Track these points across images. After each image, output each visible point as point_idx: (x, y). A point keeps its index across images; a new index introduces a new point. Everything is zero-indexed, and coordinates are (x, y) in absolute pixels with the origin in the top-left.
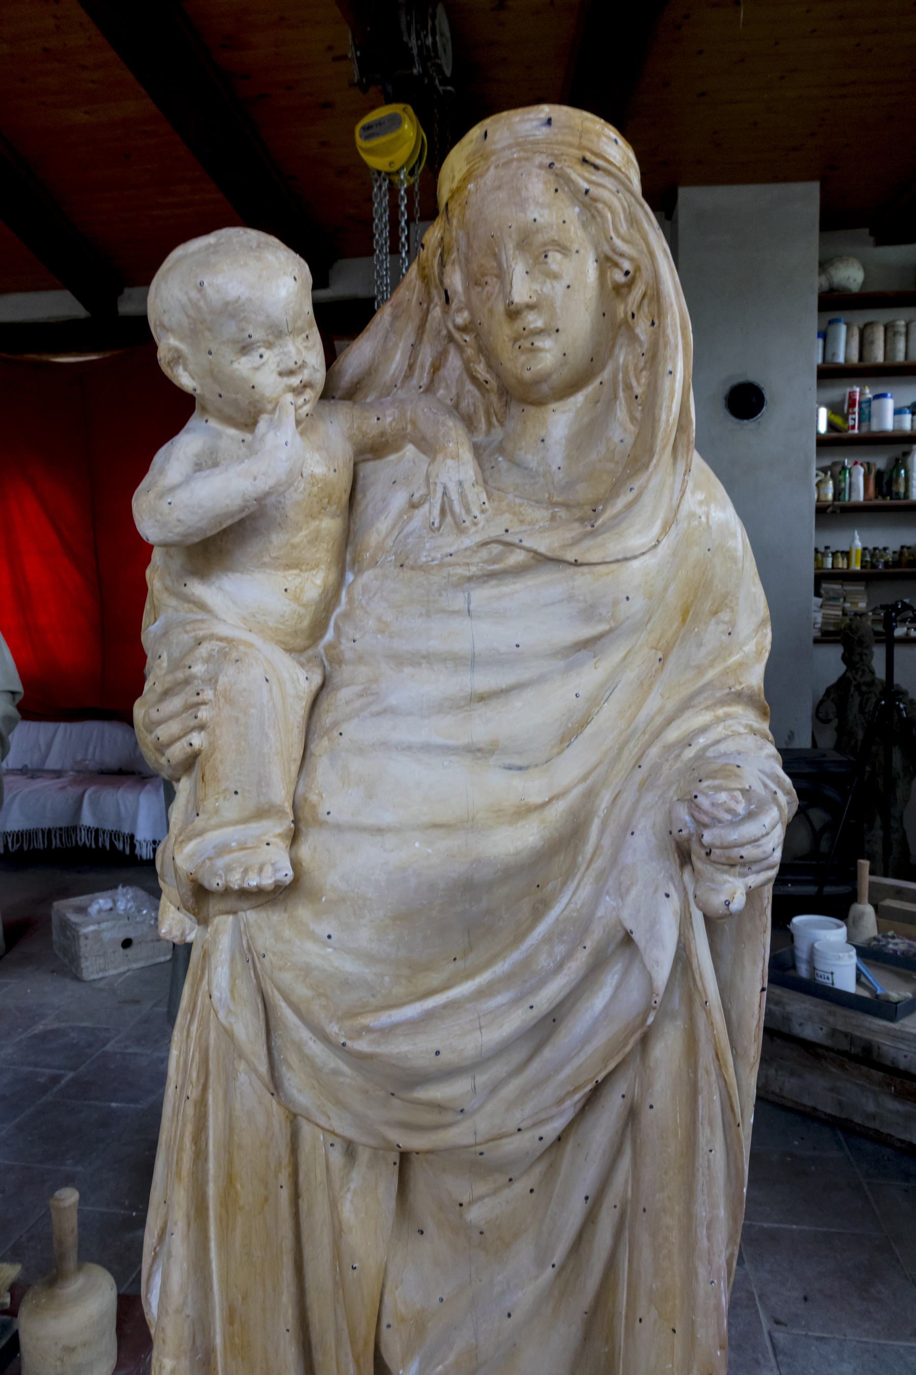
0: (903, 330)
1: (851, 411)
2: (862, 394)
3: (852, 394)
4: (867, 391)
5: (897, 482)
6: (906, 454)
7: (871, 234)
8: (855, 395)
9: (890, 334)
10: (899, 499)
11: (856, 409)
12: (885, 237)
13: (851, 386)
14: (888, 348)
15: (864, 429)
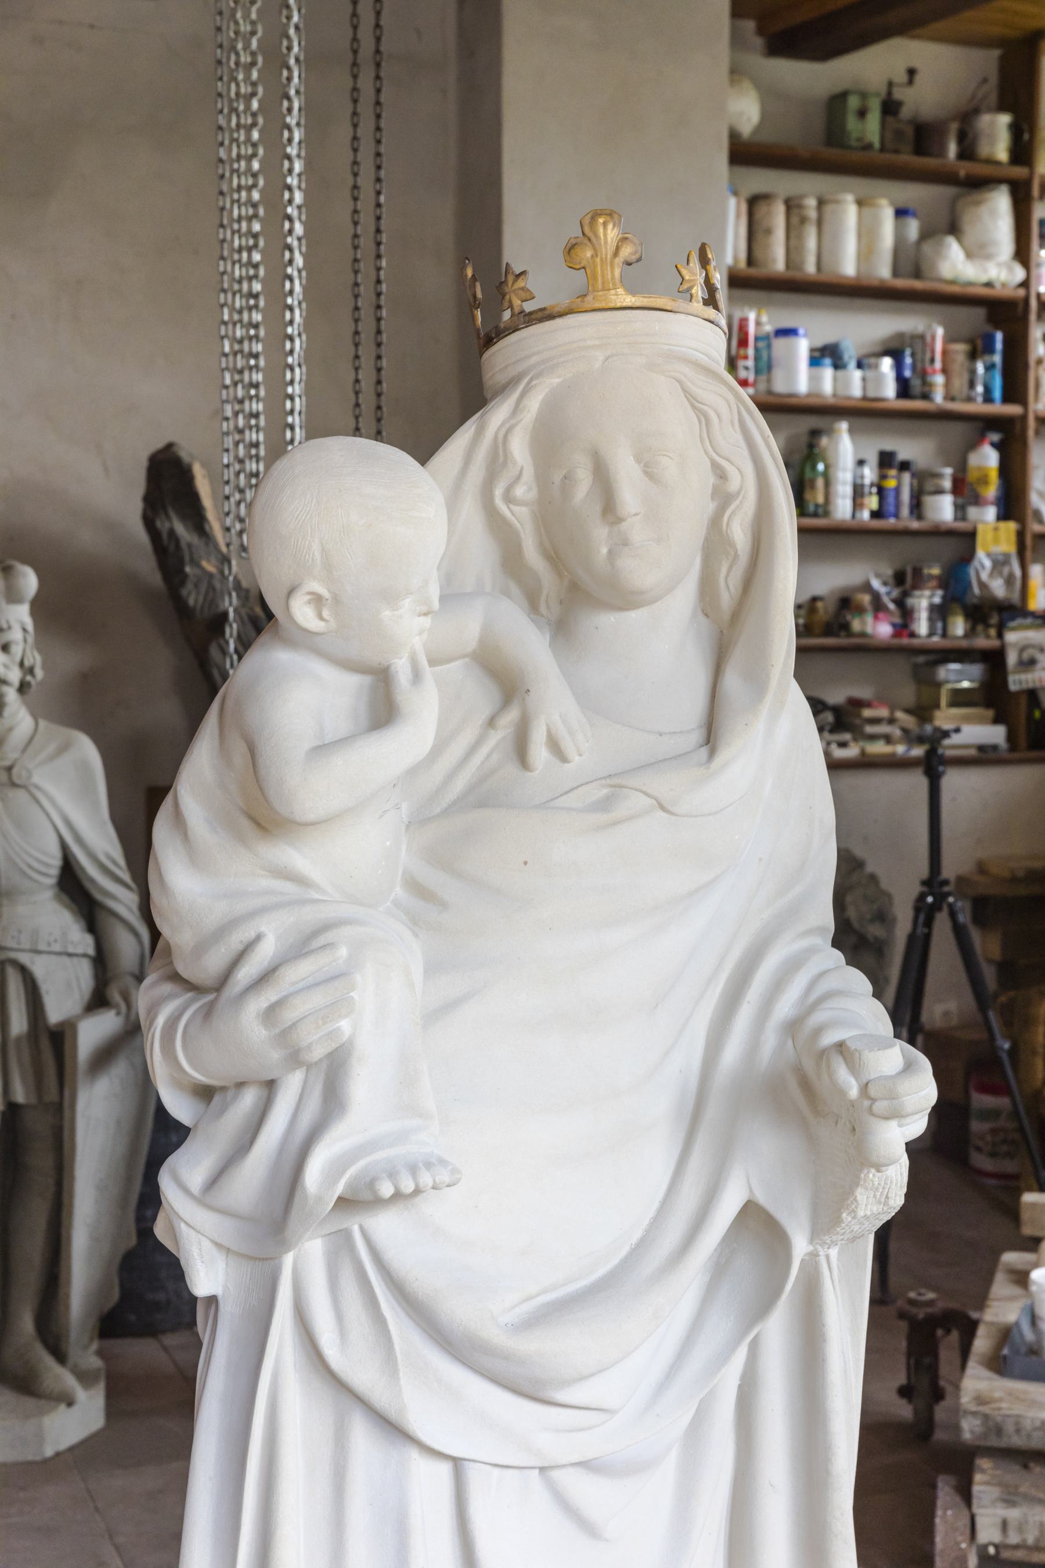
0: (813, 214)
1: (742, 352)
2: (758, 323)
3: (743, 324)
4: (764, 318)
5: (813, 487)
6: (815, 433)
7: (760, 31)
8: (747, 326)
9: (795, 220)
10: (815, 515)
11: (751, 351)
12: (784, 42)
13: (746, 309)
14: (793, 242)
15: (762, 386)
